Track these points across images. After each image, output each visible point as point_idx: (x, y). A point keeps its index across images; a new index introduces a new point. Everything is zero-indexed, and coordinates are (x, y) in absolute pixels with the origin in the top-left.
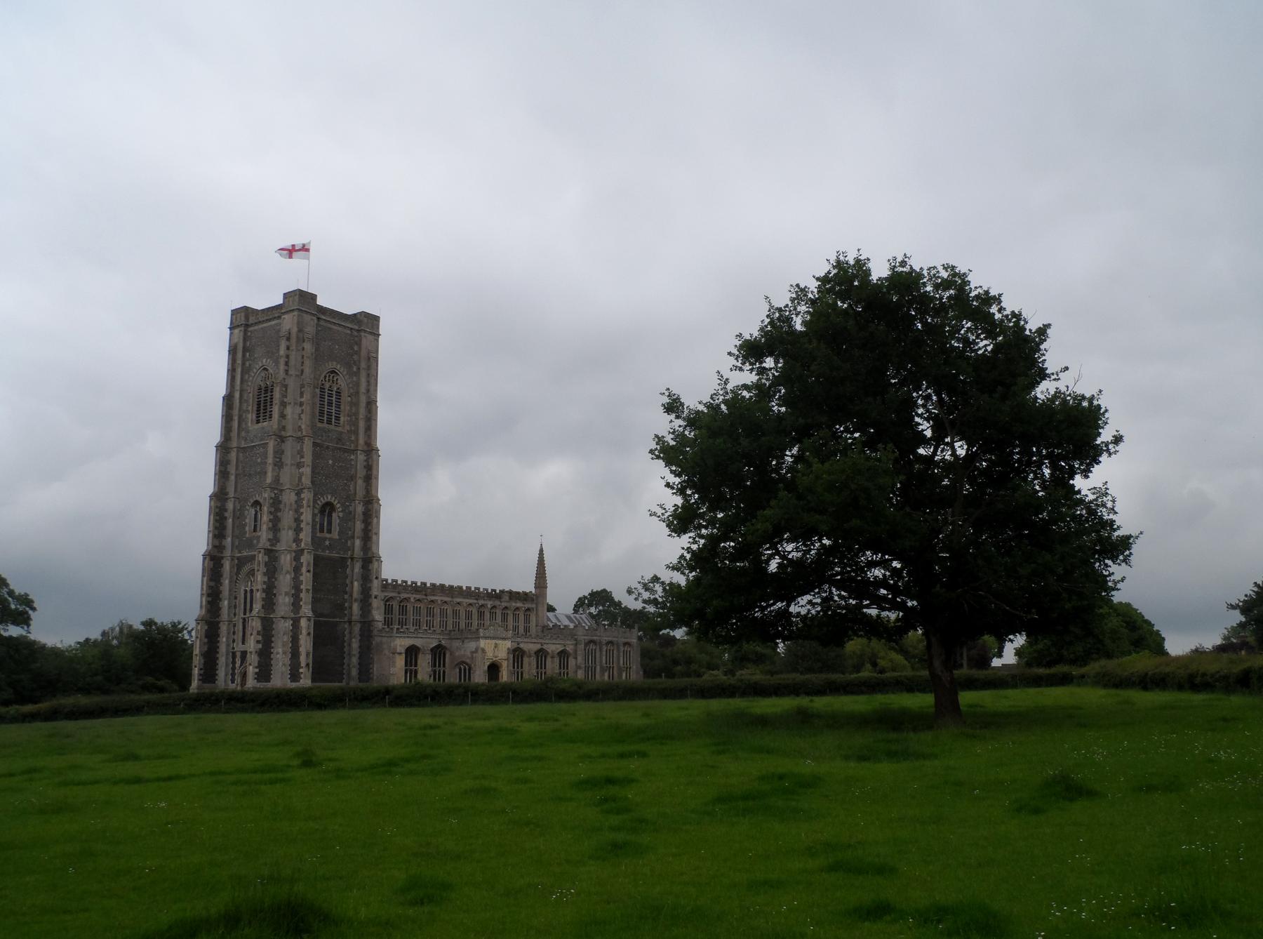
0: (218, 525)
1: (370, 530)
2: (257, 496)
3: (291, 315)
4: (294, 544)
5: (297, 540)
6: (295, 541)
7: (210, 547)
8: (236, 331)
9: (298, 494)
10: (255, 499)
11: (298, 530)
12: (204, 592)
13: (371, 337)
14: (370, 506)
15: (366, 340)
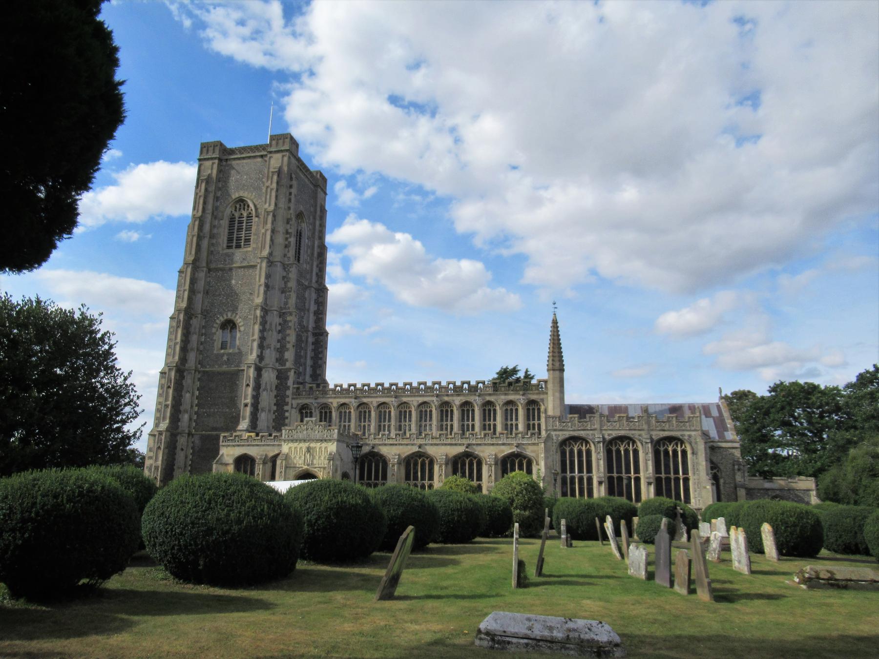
0: (184, 338)
1: (321, 359)
2: (229, 314)
3: (279, 155)
4: (278, 364)
5: (281, 360)
6: (277, 360)
7: (177, 358)
8: (208, 164)
9: (282, 315)
10: (225, 317)
11: (281, 350)
12: (169, 402)
13: (323, 195)
14: (321, 338)
15: (320, 194)
